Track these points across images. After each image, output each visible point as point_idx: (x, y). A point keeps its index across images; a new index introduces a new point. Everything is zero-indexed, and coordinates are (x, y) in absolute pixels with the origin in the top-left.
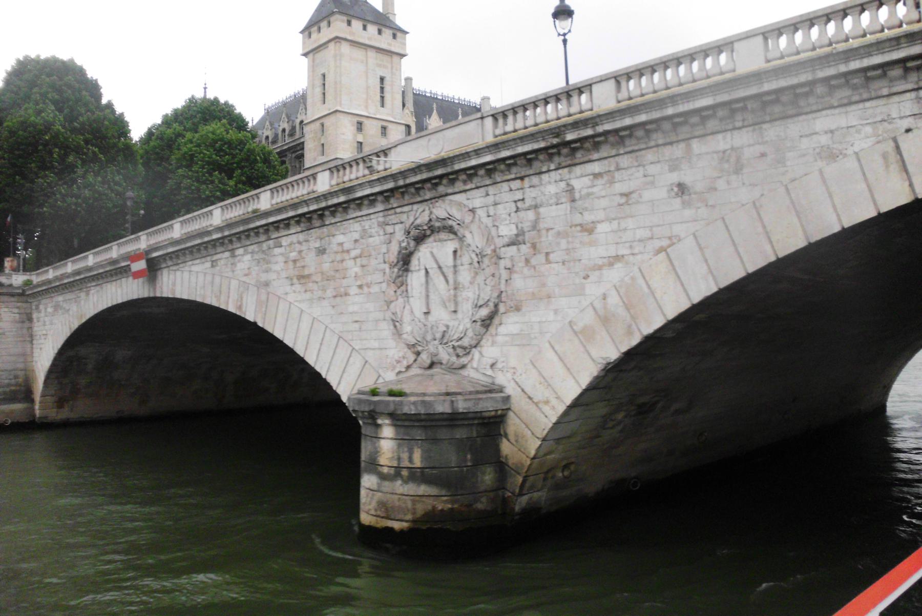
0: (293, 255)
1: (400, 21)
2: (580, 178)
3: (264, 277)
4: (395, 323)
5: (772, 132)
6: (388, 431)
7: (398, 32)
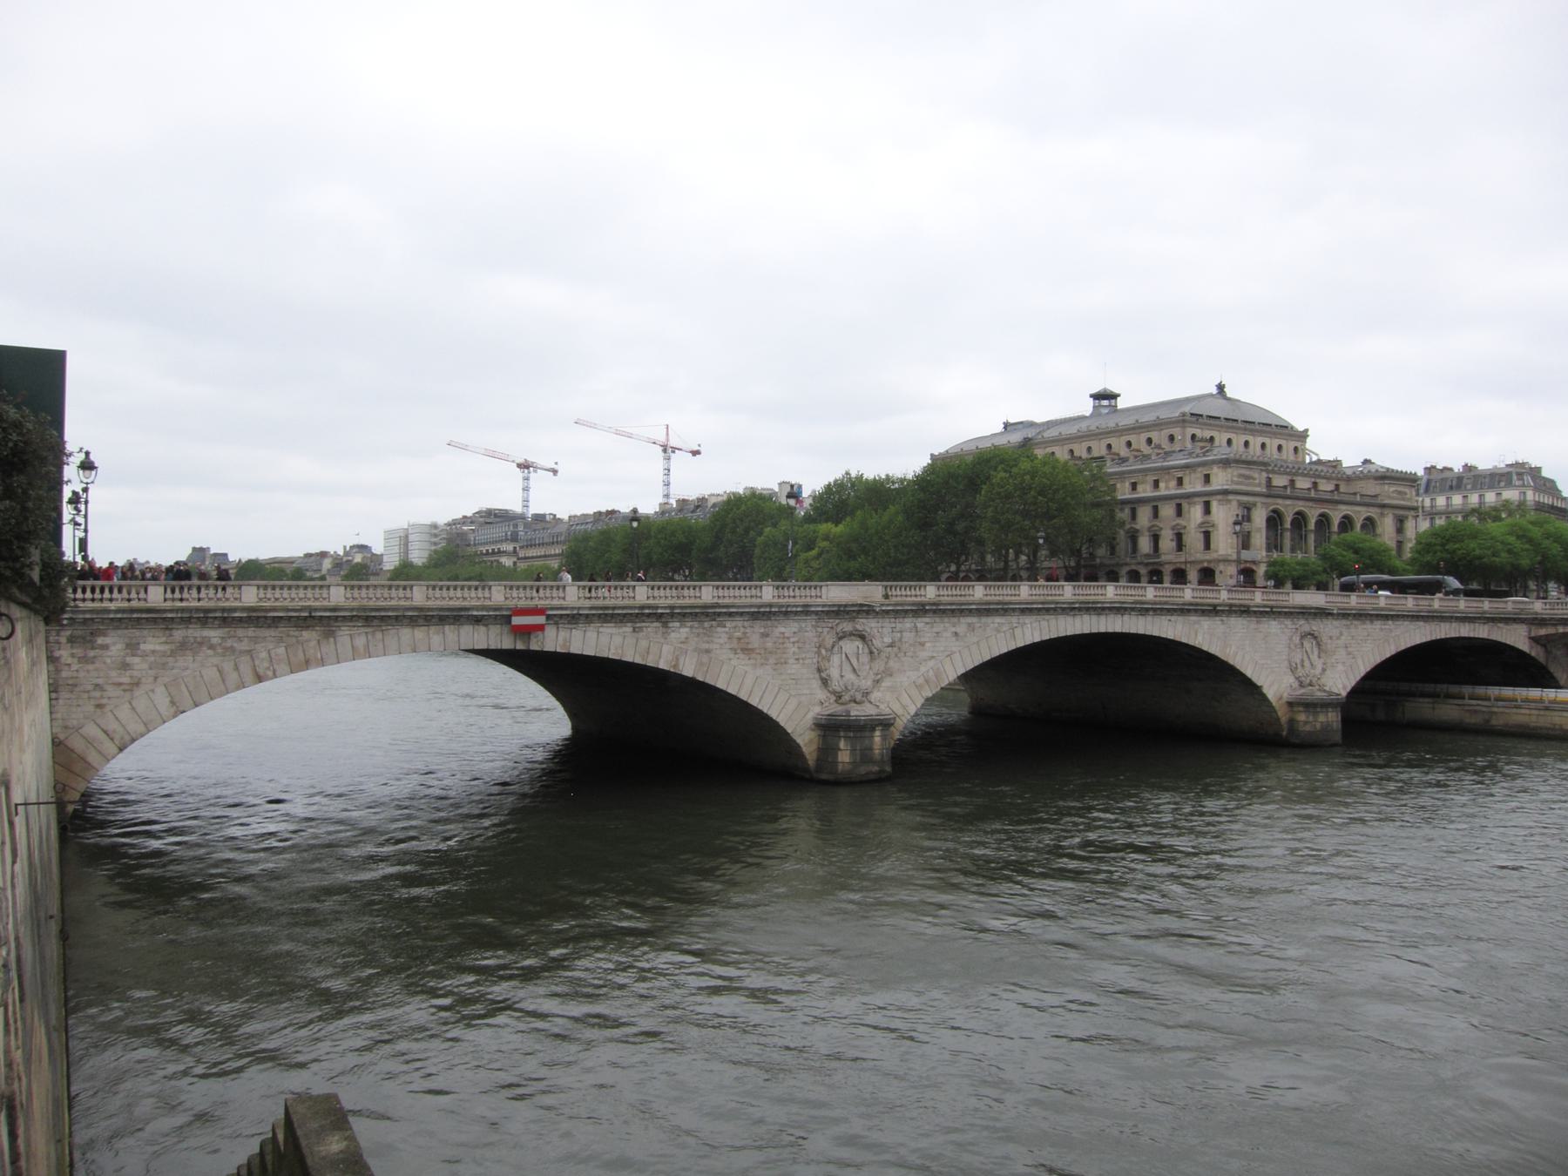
0: (738, 634)
2: (921, 623)
3: (706, 646)
5: (984, 619)
6: (878, 733)
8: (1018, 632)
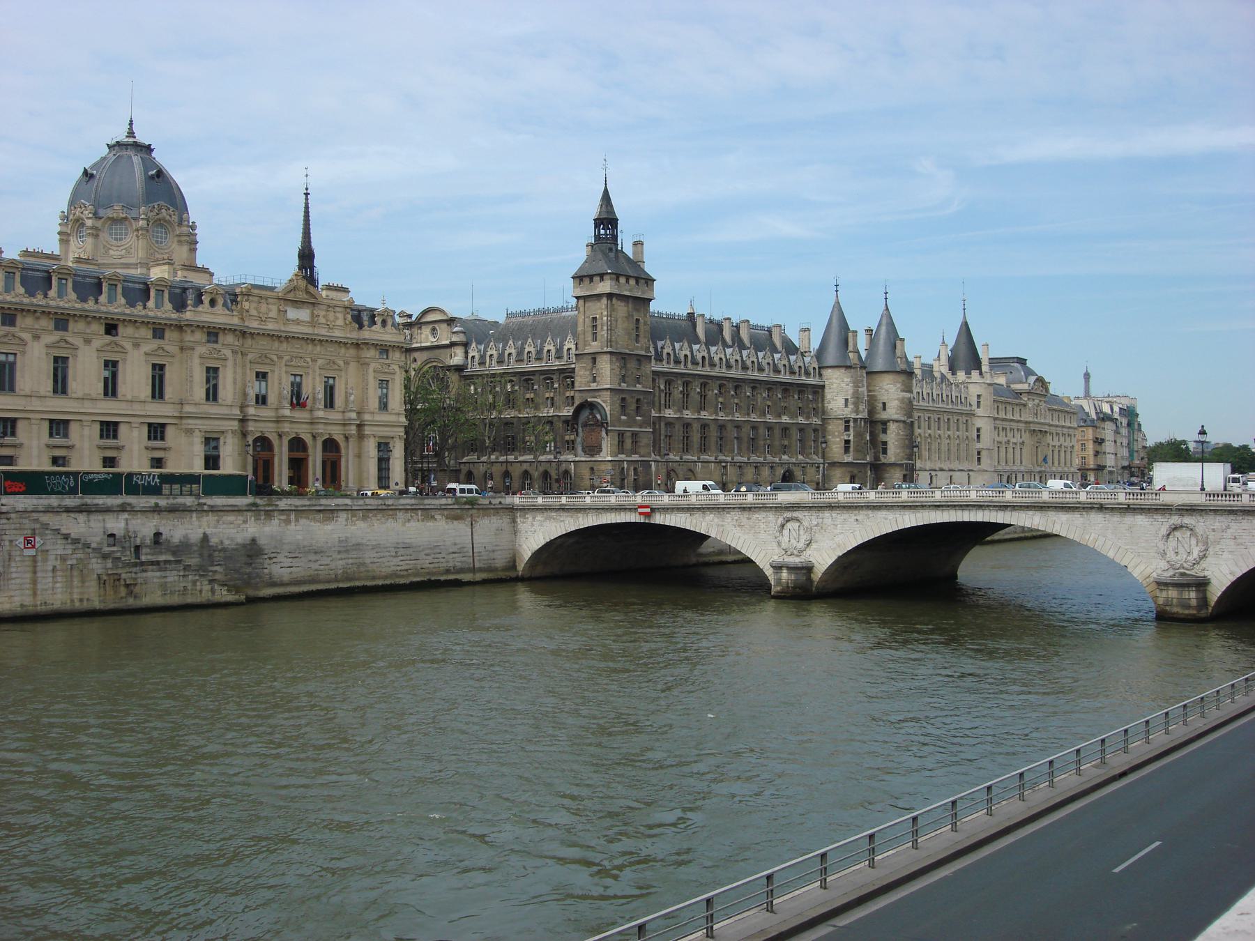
1: (649, 268)
4: (779, 543)
7: (649, 281)
8: (900, 519)
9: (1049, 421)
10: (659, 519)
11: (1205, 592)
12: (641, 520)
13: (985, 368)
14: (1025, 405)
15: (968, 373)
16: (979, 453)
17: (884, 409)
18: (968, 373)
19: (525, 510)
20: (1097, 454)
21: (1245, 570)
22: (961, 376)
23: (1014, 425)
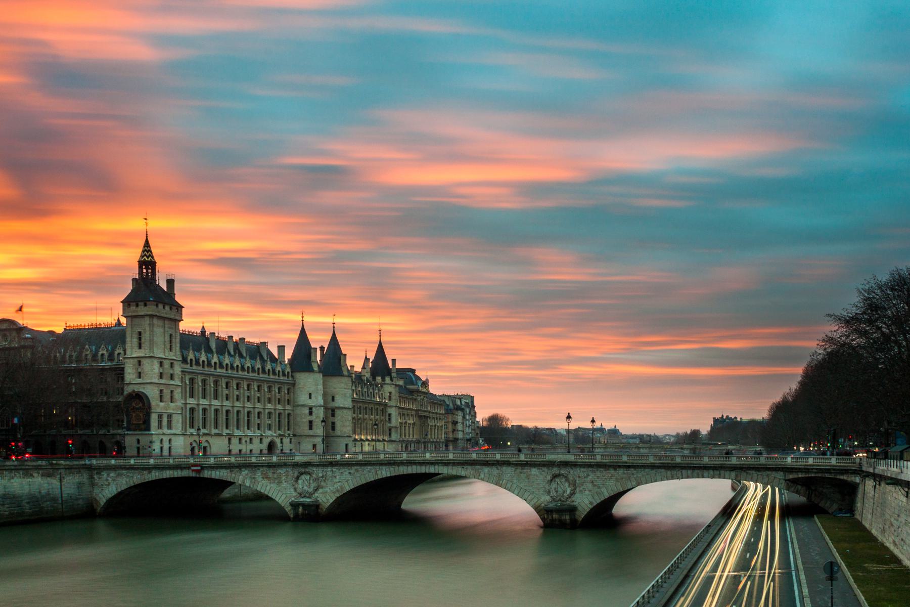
8: (379, 472)
9: (429, 409)
10: (207, 474)
11: (574, 515)
12: (194, 475)
13: (394, 375)
14: (415, 400)
15: (383, 379)
16: (390, 430)
17: (333, 399)
18: (383, 379)
19: (99, 470)
20: (454, 431)
21: (598, 501)
22: (379, 379)
23: (409, 412)
